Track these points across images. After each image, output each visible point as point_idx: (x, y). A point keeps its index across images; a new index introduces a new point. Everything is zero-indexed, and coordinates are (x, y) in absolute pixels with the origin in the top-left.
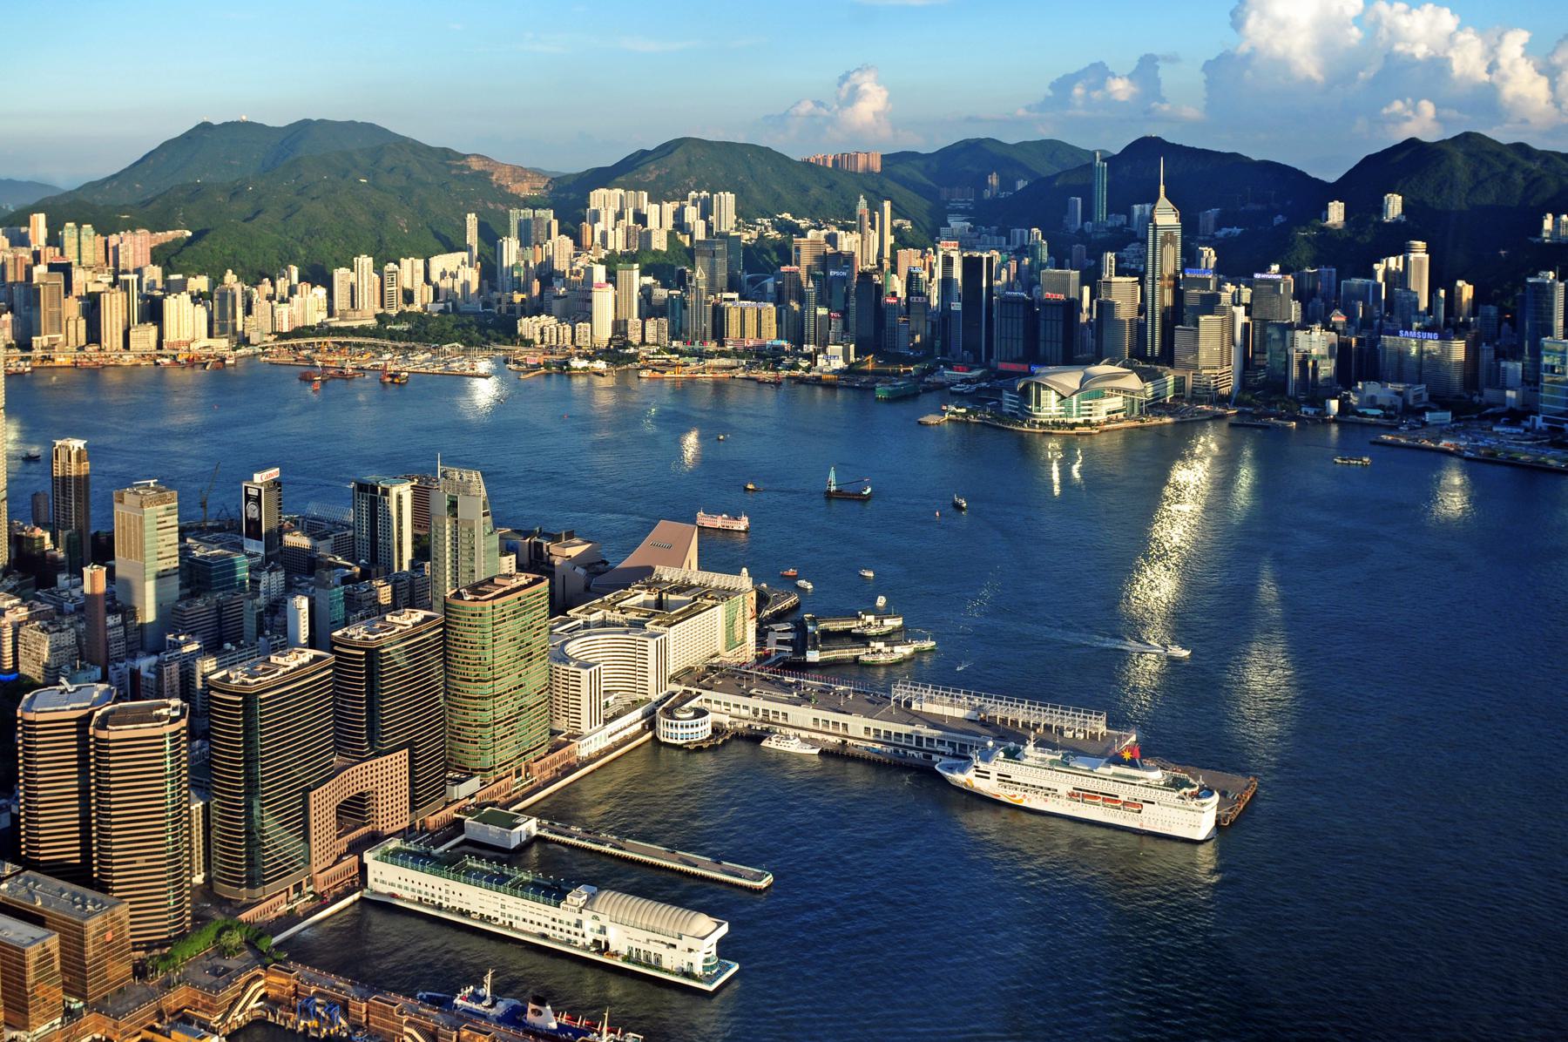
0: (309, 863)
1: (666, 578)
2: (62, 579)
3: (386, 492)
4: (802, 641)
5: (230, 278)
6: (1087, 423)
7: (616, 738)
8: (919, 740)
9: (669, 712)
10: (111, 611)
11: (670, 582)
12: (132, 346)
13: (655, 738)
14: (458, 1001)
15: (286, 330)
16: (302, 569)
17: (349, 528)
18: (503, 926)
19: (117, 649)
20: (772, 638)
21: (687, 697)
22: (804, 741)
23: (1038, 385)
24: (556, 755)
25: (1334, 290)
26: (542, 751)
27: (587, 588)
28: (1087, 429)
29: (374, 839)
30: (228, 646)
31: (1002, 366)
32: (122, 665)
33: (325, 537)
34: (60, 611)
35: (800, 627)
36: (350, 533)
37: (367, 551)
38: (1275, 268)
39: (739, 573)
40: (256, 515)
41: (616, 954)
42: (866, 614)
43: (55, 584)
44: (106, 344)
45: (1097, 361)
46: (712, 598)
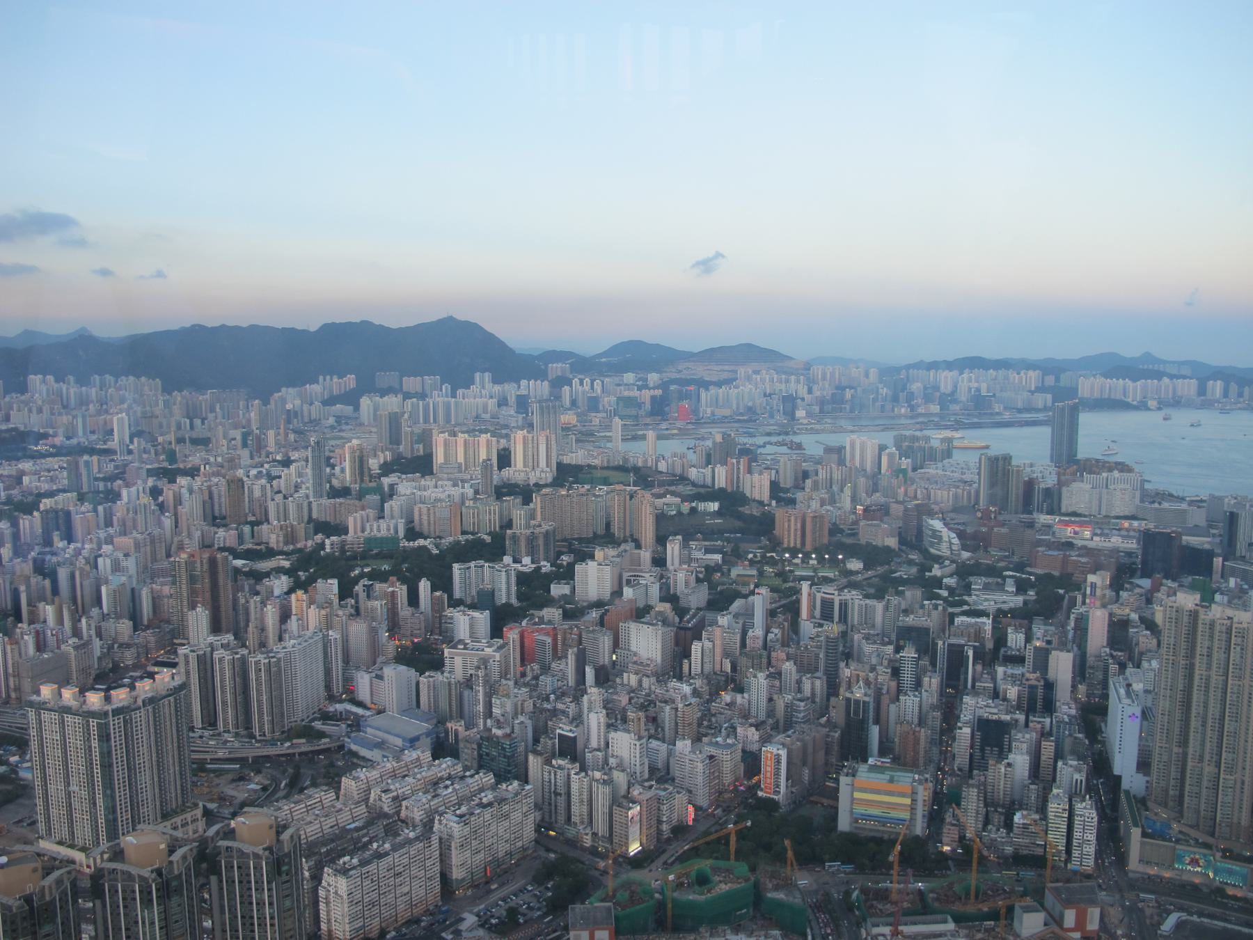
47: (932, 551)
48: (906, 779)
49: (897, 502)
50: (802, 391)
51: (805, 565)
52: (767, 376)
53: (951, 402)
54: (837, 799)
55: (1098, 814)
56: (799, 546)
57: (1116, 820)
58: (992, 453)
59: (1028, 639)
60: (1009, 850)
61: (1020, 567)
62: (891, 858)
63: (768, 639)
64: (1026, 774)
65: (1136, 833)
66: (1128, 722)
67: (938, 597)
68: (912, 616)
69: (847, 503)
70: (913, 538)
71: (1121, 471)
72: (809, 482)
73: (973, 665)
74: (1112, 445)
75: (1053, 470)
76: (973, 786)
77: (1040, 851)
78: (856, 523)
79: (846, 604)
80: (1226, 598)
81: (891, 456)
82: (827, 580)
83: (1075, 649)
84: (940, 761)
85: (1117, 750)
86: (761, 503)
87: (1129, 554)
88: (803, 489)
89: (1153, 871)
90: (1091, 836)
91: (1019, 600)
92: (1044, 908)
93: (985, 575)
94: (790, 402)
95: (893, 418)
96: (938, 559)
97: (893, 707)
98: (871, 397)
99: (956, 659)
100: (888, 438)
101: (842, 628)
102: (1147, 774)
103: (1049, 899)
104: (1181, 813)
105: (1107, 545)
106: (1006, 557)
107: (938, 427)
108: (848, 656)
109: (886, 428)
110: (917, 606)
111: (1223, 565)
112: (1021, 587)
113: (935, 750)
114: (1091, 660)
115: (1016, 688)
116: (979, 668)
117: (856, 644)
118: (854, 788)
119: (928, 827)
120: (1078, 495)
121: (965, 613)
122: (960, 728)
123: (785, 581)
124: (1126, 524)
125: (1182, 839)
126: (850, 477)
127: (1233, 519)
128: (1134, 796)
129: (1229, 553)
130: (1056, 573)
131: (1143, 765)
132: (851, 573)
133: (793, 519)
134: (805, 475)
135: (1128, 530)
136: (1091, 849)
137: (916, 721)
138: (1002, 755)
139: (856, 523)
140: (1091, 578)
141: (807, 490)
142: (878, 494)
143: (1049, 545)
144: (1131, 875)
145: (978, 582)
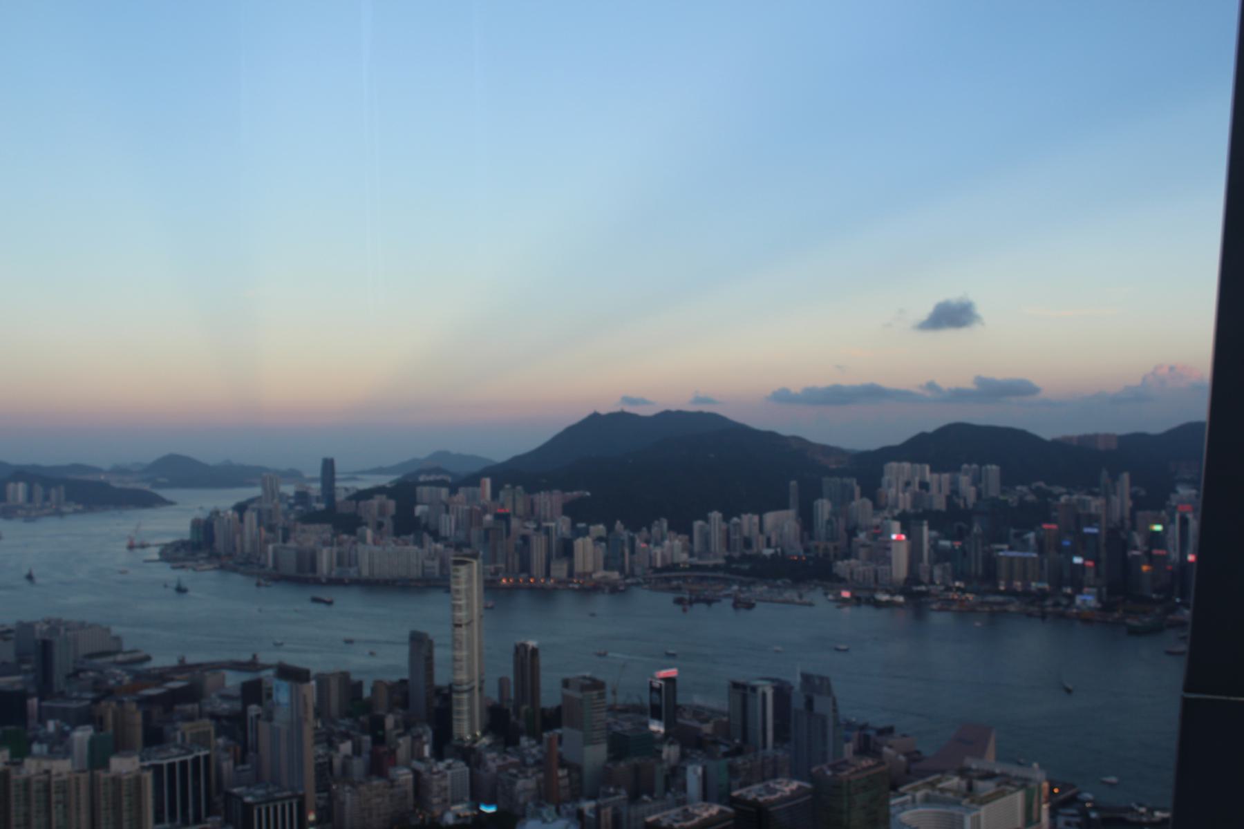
1: (974, 766)
2: (524, 741)
5: (619, 525)
10: (563, 764)
11: (977, 770)
12: (553, 573)
15: (659, 564)
16: (692, 743)
17: (723, 714)
27: (908, 772)
30: (645, 797)
32: (569, 806)
33: (706, 721)
36: (725, 719)
40: (657, 702)
42: (1140, 805)
43: (516, 743)
46: (1013, 785)
80: (45, 748)
111: (40, 707)
127: (45, 648)
129: (45, 687)
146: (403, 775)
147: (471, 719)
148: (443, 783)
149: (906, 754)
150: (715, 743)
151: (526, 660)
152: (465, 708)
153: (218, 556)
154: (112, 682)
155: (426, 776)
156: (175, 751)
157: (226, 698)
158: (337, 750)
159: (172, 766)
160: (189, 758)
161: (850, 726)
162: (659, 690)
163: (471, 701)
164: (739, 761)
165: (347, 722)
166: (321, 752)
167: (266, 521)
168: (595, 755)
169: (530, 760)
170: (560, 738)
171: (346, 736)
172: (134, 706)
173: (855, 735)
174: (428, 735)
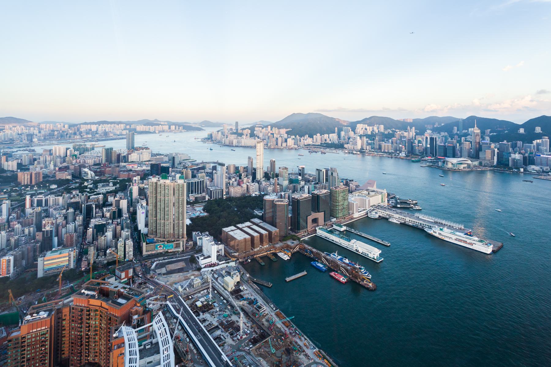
0: (307, 228)
2: (271, 179)
3: (321, 171)
4: (397, 203)
5: (297, 136)
6: (458, 169)
7: (360, 215)
8: (421, 224)
9: (370, 212)
10: (278, 184)
13: (368, 216)
14: (331, 255)
16: (307, 181)
18: (339, 244)
19: (279, 191)
20: (390, 202)
21: (374, 210)
22: (397, 221)
23: (447, 161)
24: (350, 217)
25: (522, 146)
26: (347, 216)
27: (356, 189)
28: (458, 170)
29: (318, 226)
31: (439, 157)
34: (271, 184)
35: (396, 201)
37: (318, 179)
38: (506, 141)
39: (384, 190)
41: (360, 252)
44: (279, 145)
45: (461, 157)
47: (85, 178)
48: (66, 252)
49: (72, 165)
50: (36, 132)
51: (32, 190)
52: (20, 128)
53: (96, 134)
54: (37, 267)
55: (133, 242)
56: (29, 183)
57: (140, 242)
58: (107, 147)
59: (114, 198)
60: (105, 262)
61: (115, 178)
62: (58, 280)
63: (10, 218)
64: (112, 237)
65: (144, 244)
66: (141, 214)
67: (86, 191)
68: (73, 199)
69: (52, 167)
70: (78, 175)
71: (146, 149)
72: (36, 162)
73: (95, 209)
74: (145, 143)
75: (127, 151)
76: (92, 246)
77: (115, 259)
78: (55, 173)
79: (48, 200)
81: (71, 151)
82: (41, 193)
83: (130, 198)
84: (82, 242)
85: (139, 223)
86: (13, 171)
87: (148, 170)
88: (34, 164)
89: (150, 253)
90: (132, 249)
91: (114, 188)
92: (115, 275)
93: (103, 182)
94: (30, 137)
95: (74, 139)
96: (87, 180)
97: (64, 230)
98: (65, 133)
99: (89, 209)
100: (71, 146)
101: (45, 208)
102: (148, 227)
103: (117, 272)
104: (157, 235)
105: (143, 169)
106: (110, 176)
107: (91, 141)
108: (48, 216)
109: (71, 143)
110: (76, 196)
112: (114, 184)
113: (80, 239)
114: (133, 200)
115: (109, 213)
116: (97, 210)
117: (51, 212)
118: (44, 261)
119: (77, 263)
120: (134, 157)
121: (95, 195)
122: (89, 230)
123: (21, 197)
124: (147, 163)
125: (158, 241)
126: (54, 158)
127: (174, 158)
128: (144, 234)
129: (173, 166)
130: (126, 179)
131: (146, 225)
132: (52, 189)
133: (26, 175)
134: (35, 160)
135: (148, 164)
136: (132, 253)
137: (73, 231)
138: (103, 234)
139: (55, 173)
140: (134, 178)
141: (35, 165)
142: (65, 163)
143: (124, 171)
144: (144, 256)
145: (100, 185)
146: (244, 186)
147: (260, 175)
148: (253, 188)
149: (356, 186)
150: (312, 181)
151: (273, 163)
152: (259, 172)
153: (213, 141)
154: (187, 165)
155: (249, 186)
156: (197, 179)
157: (209, 169)
158: (231, 180)
159: (195, 182)
160: (199, 181)
161: (343, 179)
162: (301, 170)
163: (260, 171)
164: (317, 185)
165: (234, 174)
166: (227, 180)
167: (223, 134)
168: (286, 183)
169: (272, 184)
170: (278, 179)
171: (234, 177)
172: (190, 170)
173: (344, 181)
174: (251, 178)
